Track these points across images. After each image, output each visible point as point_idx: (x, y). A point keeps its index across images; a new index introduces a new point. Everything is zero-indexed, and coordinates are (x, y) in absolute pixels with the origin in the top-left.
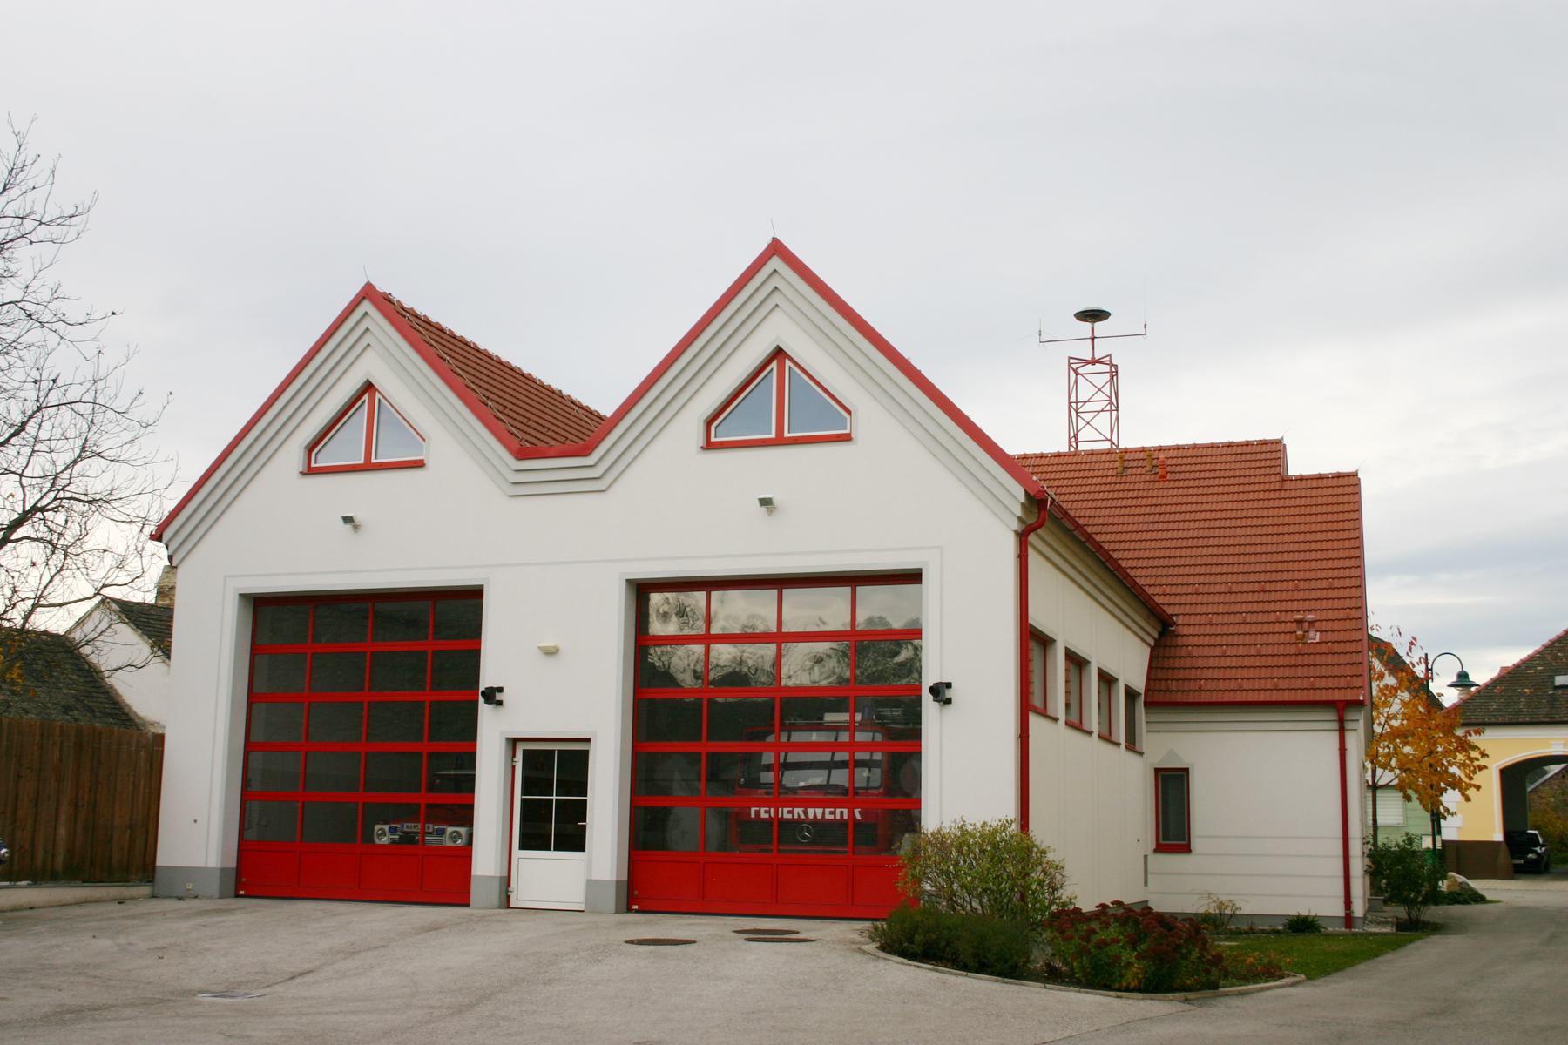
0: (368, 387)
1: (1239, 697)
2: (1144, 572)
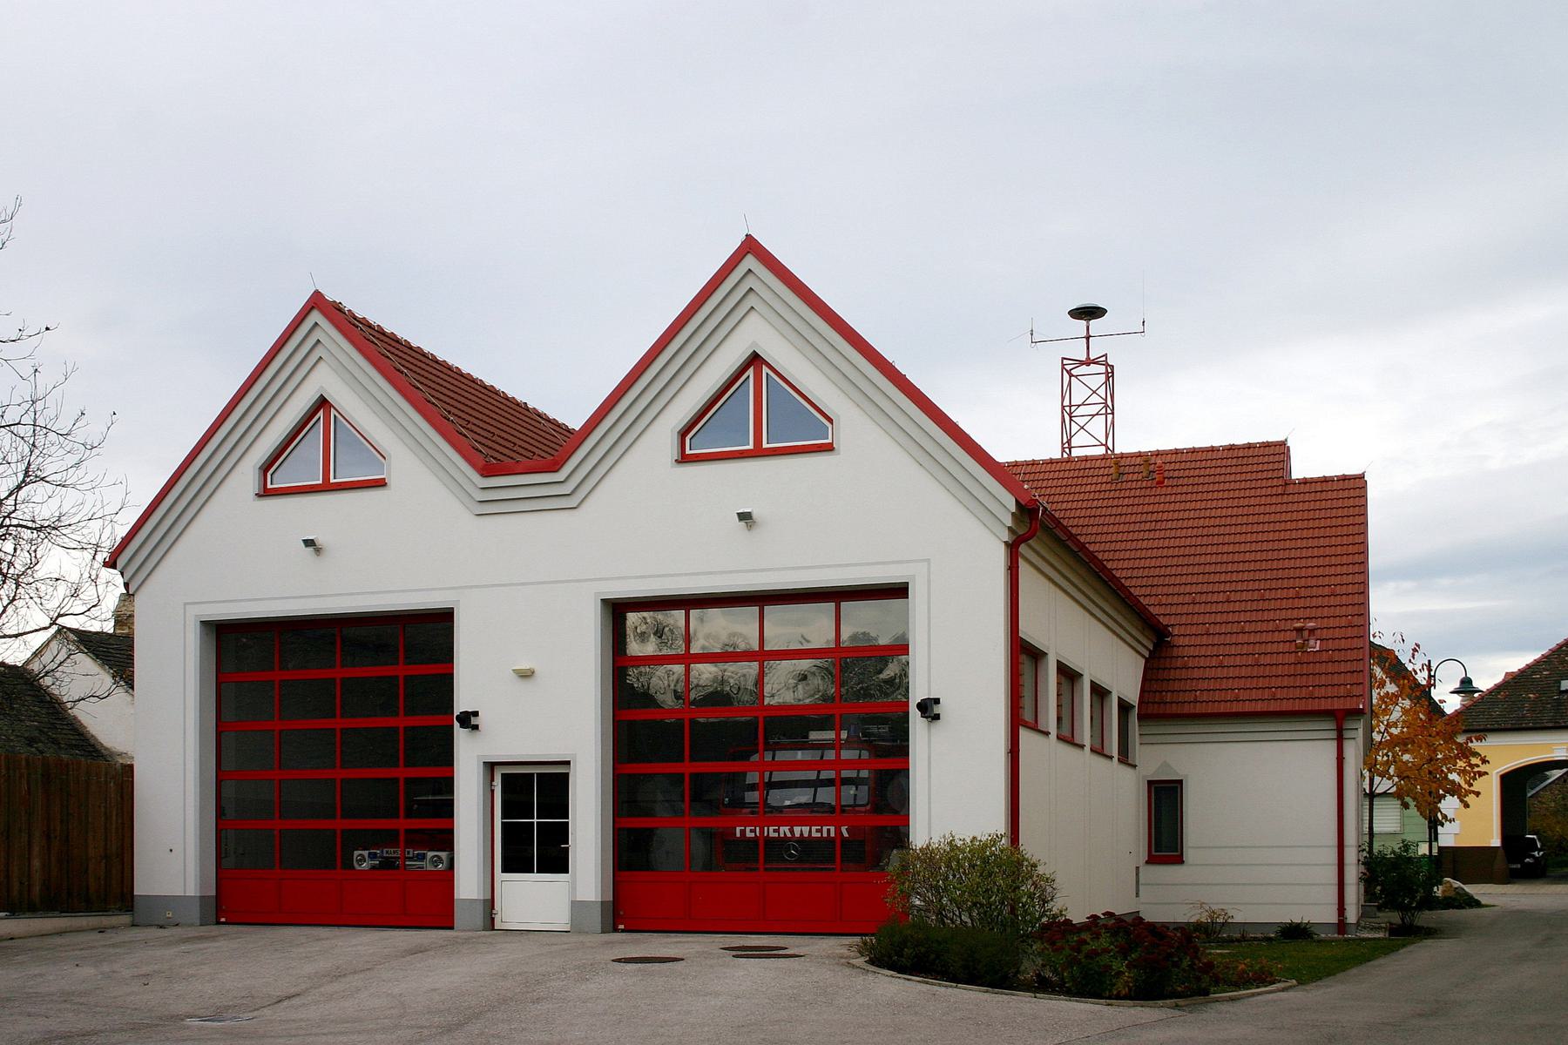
0: (323, 403)
1: (1236, 708)
2: (1139, 582)
